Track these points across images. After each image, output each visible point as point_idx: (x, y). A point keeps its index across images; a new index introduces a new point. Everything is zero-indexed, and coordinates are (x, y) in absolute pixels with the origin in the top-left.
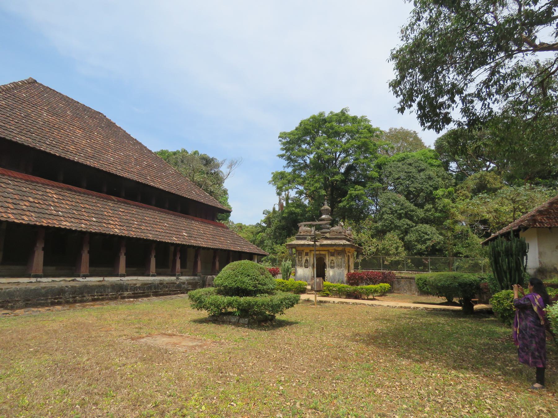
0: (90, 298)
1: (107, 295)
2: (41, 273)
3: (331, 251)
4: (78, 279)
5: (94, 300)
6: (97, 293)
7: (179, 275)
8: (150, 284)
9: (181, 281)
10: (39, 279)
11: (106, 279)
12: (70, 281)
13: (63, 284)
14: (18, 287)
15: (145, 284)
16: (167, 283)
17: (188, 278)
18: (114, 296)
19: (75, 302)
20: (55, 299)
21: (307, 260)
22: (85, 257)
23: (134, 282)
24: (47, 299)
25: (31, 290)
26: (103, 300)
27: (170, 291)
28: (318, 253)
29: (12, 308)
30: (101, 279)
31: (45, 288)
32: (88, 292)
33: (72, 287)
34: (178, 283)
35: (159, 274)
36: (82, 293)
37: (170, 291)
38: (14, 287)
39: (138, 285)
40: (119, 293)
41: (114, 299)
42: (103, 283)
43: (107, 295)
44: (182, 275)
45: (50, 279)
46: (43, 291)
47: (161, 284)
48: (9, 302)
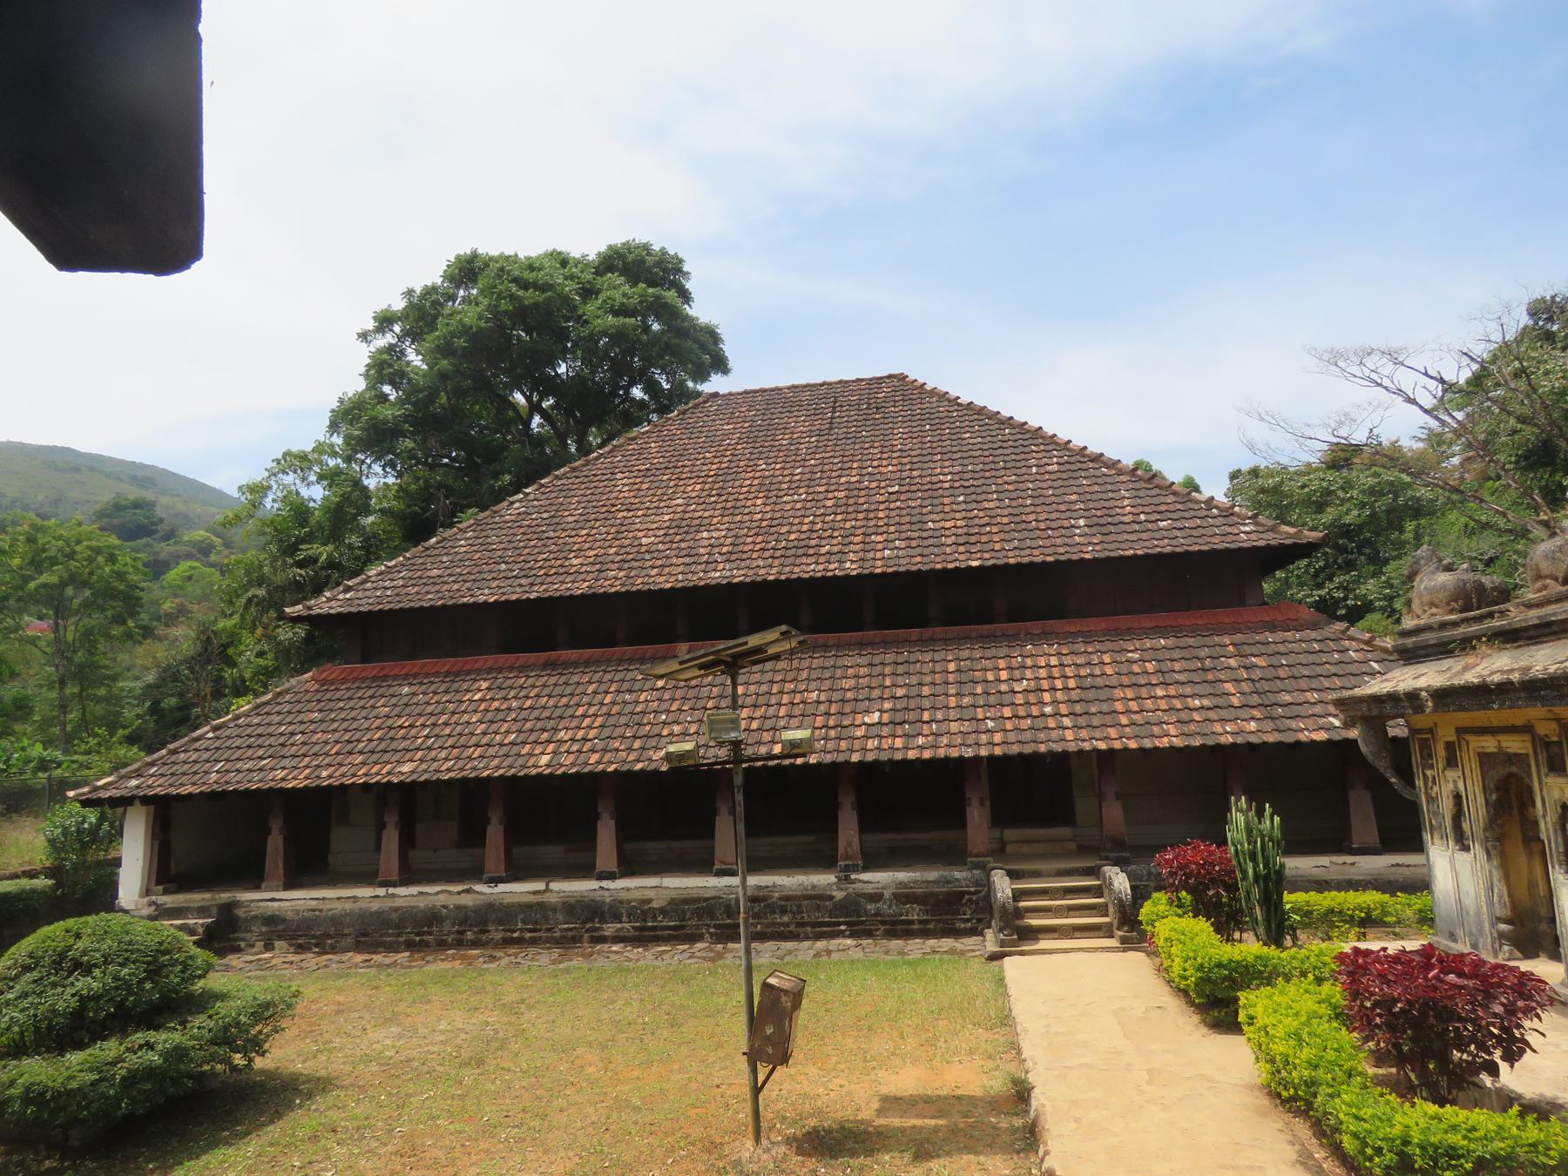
0: (498, 936)
1: (548, 930)
2: (395, 877)
3: (1543, 729)
4: (479, 887)
5: (508, 942)
6: (524, 922)
7: (847, 869)
8: (706, 900)
9: (869, 889)
10: (391, 890)
11: (555, 886)
12: (459, 893)
13: (442, 899)
14: (348, 906)
15: (686, 901)
16: (787, 898)
17: (902, 876)
18: (570, 934)
19: (460, 944)
20: (418, 934)
21: (1457, 797)
22: (495, 833)
23: (651, 894)
24: (399, 935)
25: (373, 914)
26: (533, 942)
27: (798, 925)
28: (1489, 744)
29: (333, 950)
30: (539, 886)
31: (396, 909)
32: (500, 922)
33: (458, 907)
34: (839, 895)
35: (756, 864)
36: (485, 923)
37: (803, 925)
38: (339, 906)
39: (655, 905)
40: (583, 928)
41: (568, 942)
42: (547, 898)
43: (548, 930)
44: (866, 869)
45: (414, 890)
46: (394, 915)
47: (754, 900)
48: (330, 936)
